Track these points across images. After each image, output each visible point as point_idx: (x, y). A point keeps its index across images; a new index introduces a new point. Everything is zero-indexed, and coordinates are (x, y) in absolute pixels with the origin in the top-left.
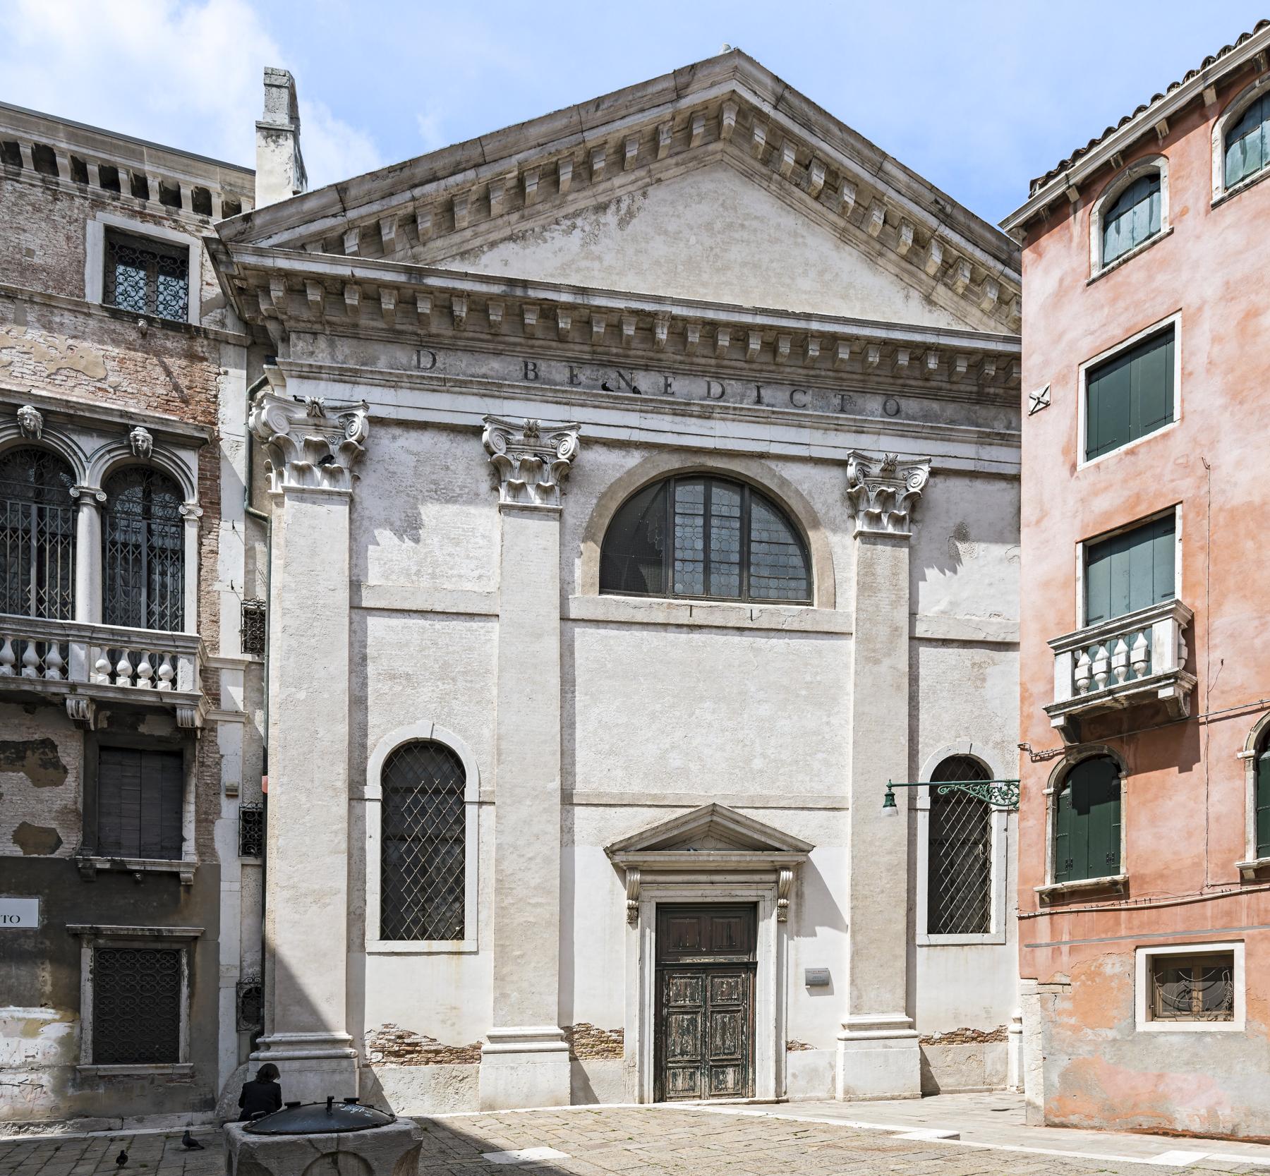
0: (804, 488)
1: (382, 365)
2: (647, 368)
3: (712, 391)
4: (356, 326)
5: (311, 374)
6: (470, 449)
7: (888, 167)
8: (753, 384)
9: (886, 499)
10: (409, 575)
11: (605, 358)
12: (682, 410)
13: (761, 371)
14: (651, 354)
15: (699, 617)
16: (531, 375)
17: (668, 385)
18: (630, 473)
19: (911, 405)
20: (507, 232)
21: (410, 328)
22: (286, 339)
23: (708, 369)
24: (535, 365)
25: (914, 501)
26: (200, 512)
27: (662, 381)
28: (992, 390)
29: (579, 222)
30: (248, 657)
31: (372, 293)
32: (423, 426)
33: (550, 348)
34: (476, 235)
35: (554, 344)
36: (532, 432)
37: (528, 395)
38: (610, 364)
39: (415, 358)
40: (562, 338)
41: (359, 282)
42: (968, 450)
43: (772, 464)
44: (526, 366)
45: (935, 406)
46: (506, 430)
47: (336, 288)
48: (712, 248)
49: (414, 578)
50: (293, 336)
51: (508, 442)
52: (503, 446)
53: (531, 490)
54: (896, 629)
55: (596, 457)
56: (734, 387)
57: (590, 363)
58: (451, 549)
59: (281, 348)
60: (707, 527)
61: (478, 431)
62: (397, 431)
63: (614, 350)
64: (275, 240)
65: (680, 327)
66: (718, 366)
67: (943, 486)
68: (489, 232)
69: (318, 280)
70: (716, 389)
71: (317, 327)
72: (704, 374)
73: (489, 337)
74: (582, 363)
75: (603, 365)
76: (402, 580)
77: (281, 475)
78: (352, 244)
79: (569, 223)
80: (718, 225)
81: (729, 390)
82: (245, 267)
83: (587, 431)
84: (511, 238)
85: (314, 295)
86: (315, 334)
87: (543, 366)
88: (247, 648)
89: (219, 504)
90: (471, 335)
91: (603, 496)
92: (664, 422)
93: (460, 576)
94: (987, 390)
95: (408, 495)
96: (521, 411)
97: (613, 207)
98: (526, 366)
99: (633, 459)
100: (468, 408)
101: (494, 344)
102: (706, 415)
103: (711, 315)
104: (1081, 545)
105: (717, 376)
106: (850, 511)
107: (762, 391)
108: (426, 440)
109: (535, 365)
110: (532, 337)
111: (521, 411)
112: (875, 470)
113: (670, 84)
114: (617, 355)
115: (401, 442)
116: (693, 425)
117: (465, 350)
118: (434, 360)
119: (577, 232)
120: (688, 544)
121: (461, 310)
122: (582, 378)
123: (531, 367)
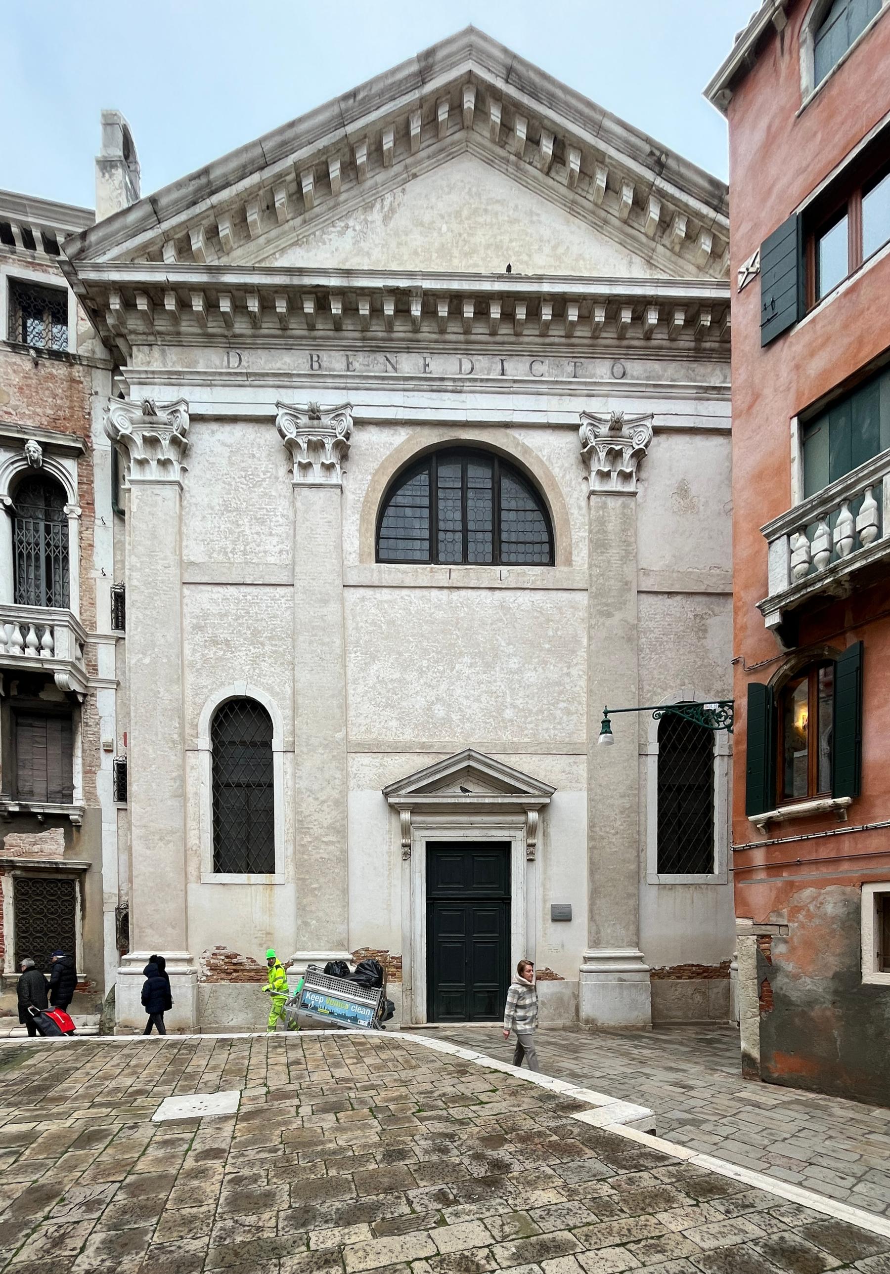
10: (226, 553)
26: (79, 511)
49: (231, 555)
58: (258, 528)
60: (464, 499)
70: (466, 366)
76: (221, 558)
89: (93, 504)
93: (265, 552)
97: (378, 206)
103: (455, 285)
104: (795, 420)
113: (414, 68)
120: (450, 515)
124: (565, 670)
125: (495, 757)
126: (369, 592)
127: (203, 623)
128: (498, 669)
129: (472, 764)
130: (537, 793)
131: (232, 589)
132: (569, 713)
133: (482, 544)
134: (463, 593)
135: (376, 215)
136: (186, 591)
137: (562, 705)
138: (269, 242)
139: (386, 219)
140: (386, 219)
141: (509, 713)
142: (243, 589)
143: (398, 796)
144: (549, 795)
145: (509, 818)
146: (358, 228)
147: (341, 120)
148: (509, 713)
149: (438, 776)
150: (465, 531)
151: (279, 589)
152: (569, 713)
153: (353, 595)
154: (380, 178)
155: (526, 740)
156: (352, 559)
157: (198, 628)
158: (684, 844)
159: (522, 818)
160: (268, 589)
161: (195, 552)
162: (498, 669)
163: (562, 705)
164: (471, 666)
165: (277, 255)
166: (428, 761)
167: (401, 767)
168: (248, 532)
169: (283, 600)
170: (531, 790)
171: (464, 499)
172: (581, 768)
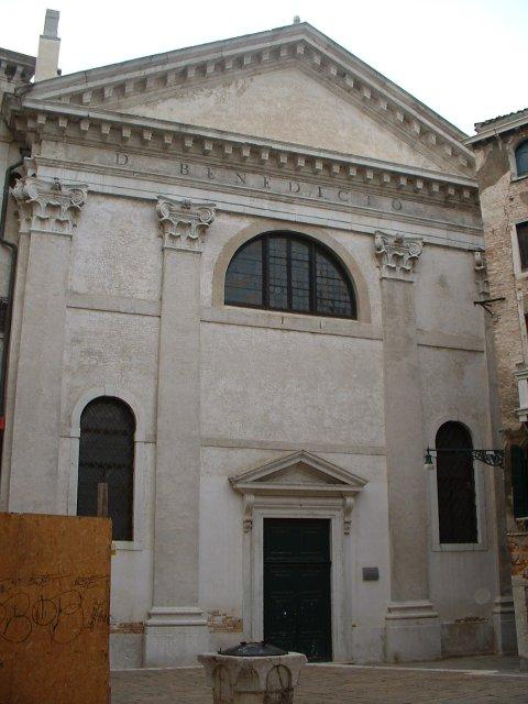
0: (349, 248)
1: (95, 161)
2: (253, 172)
4: (83, 139)
5: (54, 164)
6: (147, 211)
7: (388, 84)
9: (398, 258)
12: (275, 198)
15: (288, 324)
17: (266, 183)
18: (244, 232)
19: (408, 205)
22: (39, 142)
25: (413, 259)
31: (96, 124)
32: (118, 197)
36: (186, 206)
37: (183, 183)
38: (232, 168)
40: (206, 153)
41: (88, 118)
42: (442, 233)
43: (329, 232)
45: (421, 206)
46: (170, 203)
47: (75, 121)
50: (43, 142)
51: (170, 210)
52: (167, 213)
53: (183, 238)
54: (411, 339)
55: (221, 221)
56: (304, 186)
59: (34, 148)
60: (289, 267)
61: (154, 202)
62: (102, 199)
64: (43, 97)
65: (275, 154)
67: (429, 251)
69: (67, 116)
70: (295, 187)
72: (287, 178)
74: (215, 166)
75: (228, 168)
77: (29, 221)
78: (87, 98)
80: (293, 99)
82: (25, 108)
83: (220, 206)
85: (63, 123)
87: (191, 167)
91: (227, 246)
92: (266, 204)
96: (178, 193)
97: (234, 84)
99: (245, 224)
100: (148, 189)
101: (165, 152)
102: (290, 201)
106: (378, 264)
108: (119, 205)
111: (178, 193)
112: (391, 241)
115: (102, 205)
116: (281, 207)
117: (146, 155)
121: (148, 136)
124: (368, 394)
125: (318, 454)
126: (219, 327)
127: (80, 338)
129: (303, 460)
130: (353, 483)
132: (371, 424)
133: (301, 299)
134: (292, 333)
135: (232, 90)
136: (69, 313)
137: (367, 419)
138: (155, 94)
139: (239, 93)
140: (239, 93)
142: (117, 315)
144: (362, 485)
145: (330, 501)
147: (221, 49)
148: (327, 422)
150: (290, 288)
151: (146, 318)
152: (371, 424)
154: (236, 73)
155: (340, 443)
156: (207, 301)
158: (457, 522)
159: (340, 501)
161: (79, 285)
163: (367, 419)
164: (298, 386)
165: (160, 101)
166: (271, 457)
167: (243, 461)
168: (122, 274)
170: (350, 482)
171: (289, 267)
172: (382, 465)
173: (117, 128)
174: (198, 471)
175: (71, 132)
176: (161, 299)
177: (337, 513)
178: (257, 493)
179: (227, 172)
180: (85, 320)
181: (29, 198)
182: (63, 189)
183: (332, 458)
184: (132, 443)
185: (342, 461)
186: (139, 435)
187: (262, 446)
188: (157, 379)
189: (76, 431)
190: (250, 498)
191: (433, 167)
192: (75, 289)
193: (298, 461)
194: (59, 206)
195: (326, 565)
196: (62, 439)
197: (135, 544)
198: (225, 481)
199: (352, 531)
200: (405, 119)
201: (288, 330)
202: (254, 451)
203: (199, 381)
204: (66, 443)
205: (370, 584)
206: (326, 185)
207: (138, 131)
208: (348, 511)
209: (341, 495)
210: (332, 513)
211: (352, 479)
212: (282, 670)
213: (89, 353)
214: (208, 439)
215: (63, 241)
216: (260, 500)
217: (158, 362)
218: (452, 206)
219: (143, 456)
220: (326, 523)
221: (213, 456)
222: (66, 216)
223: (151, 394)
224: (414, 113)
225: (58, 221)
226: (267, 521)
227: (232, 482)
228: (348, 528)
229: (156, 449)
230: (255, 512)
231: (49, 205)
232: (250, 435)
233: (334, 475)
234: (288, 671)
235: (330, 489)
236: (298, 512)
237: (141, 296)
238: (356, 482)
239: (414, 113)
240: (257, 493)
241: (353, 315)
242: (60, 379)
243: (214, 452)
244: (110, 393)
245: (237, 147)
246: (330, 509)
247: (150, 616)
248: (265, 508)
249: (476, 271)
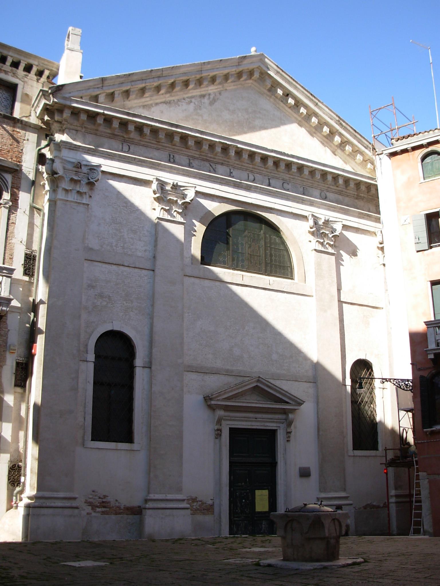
2: (222, 164)
3: (250, 178)
4: (97, 130)
8: (267, 177)
11: (205, 157)
13: (271, 173)
14: (225, 159)
16: (172, 160)
20: (163, 100)
21: (121, 134)
23: (248, 168)
24: (174, 156)
27: (229, 170)
28: (362, 195)
29: (193, 100)
30: (26, 278)
33: (181, 150)
34: (151, 100)
35: (184, 149)
38: (207, 160)
39: (121, 146)
44: (170, 156)
48: (248, 119)
57: (197, 159)
63: (209, 155)
66: (253, 168)
68: (156, 99)
71: (79, 129)
72: (246, 170)
73: (156, 142)
74: (194, 158)
75: (203, 160)
79: (189, 100)
80: (250, 110)
81: (256, 178)
84: (165, 103)
86: (77, 131)
88: (25, 274)
90: (148, 141)
94: (361, 195)
95: (113, 207)
97: (207, 97)
98: (170, 156)
105: (252, 172)
107: (270, 181)
109: (174, 156)
110: (174, 145)
114: (211, 157)
117: (143, 145)
118: (129, 148)
119: (192, 104)
122: (194, 164)
123: (172, 157)
125: (270, 380)
126: (197, 281)
128: (268, 332)
130: (294, 403)
131: (114, 267)
136: (86, 264)
141: (275, 357)
142: (122, 268)
143: (218, 400)
144: (300, 404)
146: (196, 103)
148: (275, 357)
149: (240, 390)
151: (144, 271)
153: (188, 281)
157: (91, 286)
160: (136, 270)
162: (268, 332)
169: (146, 278)
173: (124, 124)
174: (183, 390)
175: (90, 126)
176: (154, 257)
177: (281, 425)
178: (227, 408)
179: (203, 163)
180: (99, 271)
181: (56, 173)
182: (83, 167)
183: (278, 383)
184: (132, 368)
185: (286, 386)
186: (139, 361)
187: (228, 373)
188: (152, 318)
189: (91, 357)
190: (221, 413)
191: (348, 168)
192: (90, 246)
193: (255, 384)
194: (80, 181)
195: (274, 464)
196: (81, 363)
197: (135, 446)
198: (201, 397)
199: (292, 439)
200: (330, 131)
201: (247, 286)
202: (222, 377)
203: (183, 321)
204: (83, 366)
205: (304, 480)
206: (273, 177)
207: (140, 128)
208: (290, 424)
209: (285, 412)
210: (278, 425)
211: (293, 400)
212: (336, 522)
213: (101, 296)
214: (189, 366)
215: (81, 208)
216: (227, 414)
217: (153, 306)
218: (363, 198)
219: (140, 376)
220: (273, 433)
221: (191, 378)
222: (84, 189)
223: (146, 330)
224: (337, 127)
225: (78, 192)
226: (232, 431)
227: (207, 399)
228: (289, 437)
229: (151, 371)
230: (223, 422)
231: (72, 180)
232: (219, 364)
233: (281, 396)
234: (339, 521)
235: (277, 406)
236: (253, 423)
237: (140, 254)
238: (296, 401)
239: (337, 127)
240: (227, 408)
241: (292, 279)
242: (80, 316)
243: (194, 376)
244: (117, 328)
245: (212, 145)
246: (277, 422)
247: (146, 501)
248: (230, 420)
249: (378, 247)
